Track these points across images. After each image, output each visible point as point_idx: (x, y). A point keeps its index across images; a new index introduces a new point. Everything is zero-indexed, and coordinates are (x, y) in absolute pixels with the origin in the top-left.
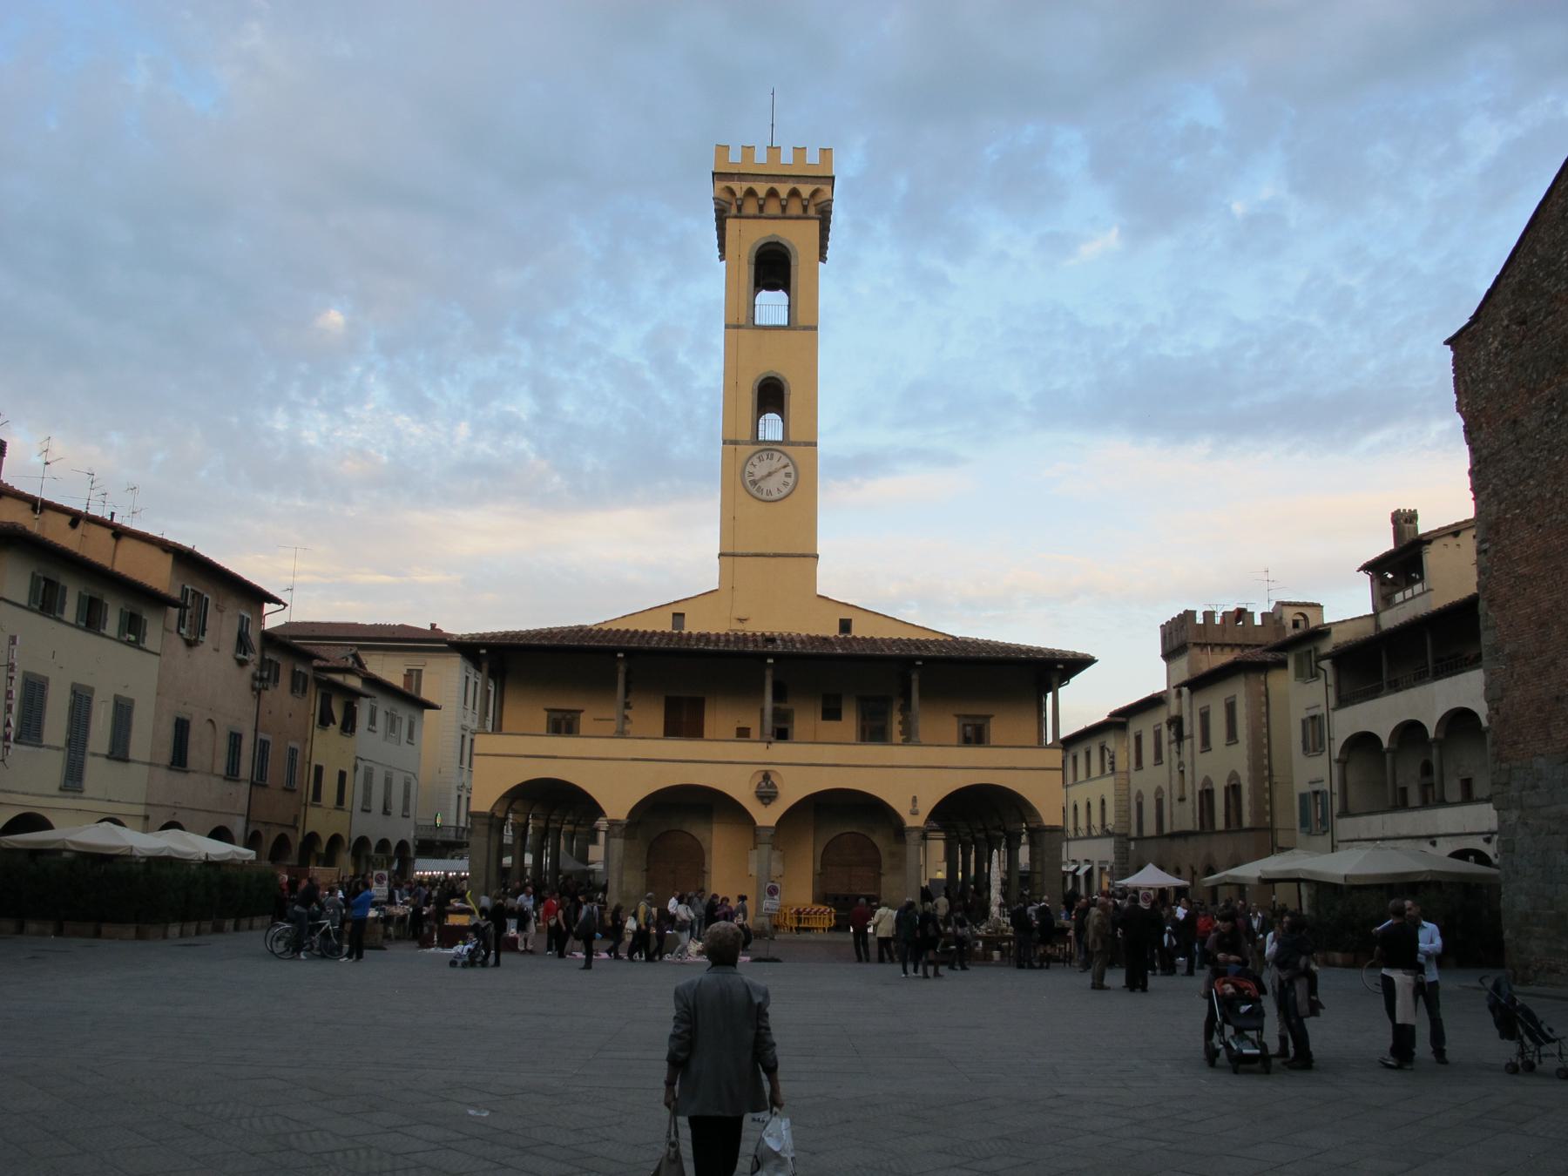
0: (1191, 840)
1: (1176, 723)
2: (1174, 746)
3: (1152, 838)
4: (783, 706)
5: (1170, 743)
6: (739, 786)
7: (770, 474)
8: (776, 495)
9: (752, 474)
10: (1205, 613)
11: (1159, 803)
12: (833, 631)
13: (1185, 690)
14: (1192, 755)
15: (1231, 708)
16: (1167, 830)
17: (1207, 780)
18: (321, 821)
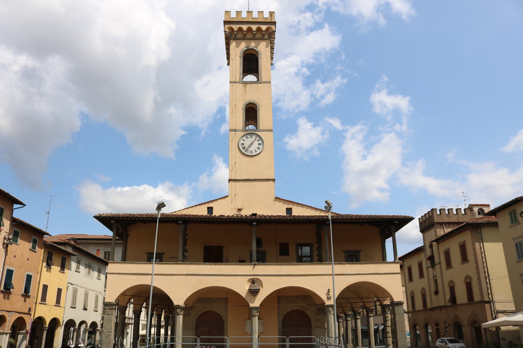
1: (431, 258)
2: (430, 269)
3: (422, 311)
4: (261, 249)
5: (427, 268)
6: (242, 287)
7: (251, 144)
8: (254, 153)
9: (243, 144)
10: (440, 210)
11: (424, 296)
12: (284, 213)
13: (435, 244)
14: (441, 271)
15: (463, 248)
17: (451, 282)
18: (47, 312)
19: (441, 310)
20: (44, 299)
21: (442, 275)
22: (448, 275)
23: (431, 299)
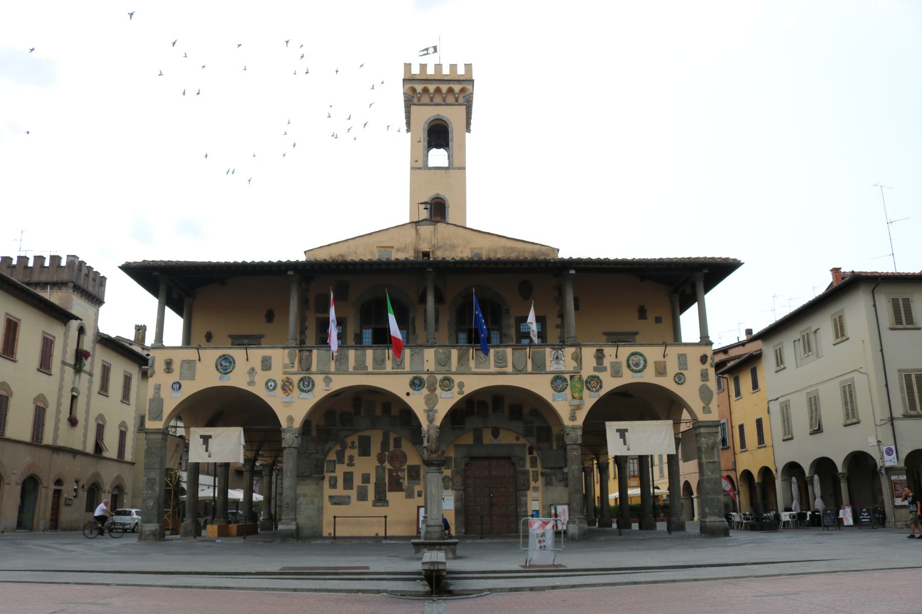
0: (79, 458)
2: (70, 371)
14: (89, 389)
16: (48, 439)
17: (101, 417)
19: (74, 457)
20: (743, 445)
21: (89, 397)
22: (99, 405)
23: (56, 429)
